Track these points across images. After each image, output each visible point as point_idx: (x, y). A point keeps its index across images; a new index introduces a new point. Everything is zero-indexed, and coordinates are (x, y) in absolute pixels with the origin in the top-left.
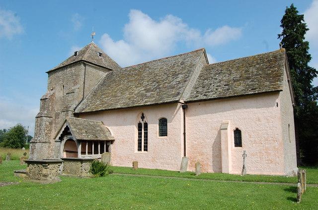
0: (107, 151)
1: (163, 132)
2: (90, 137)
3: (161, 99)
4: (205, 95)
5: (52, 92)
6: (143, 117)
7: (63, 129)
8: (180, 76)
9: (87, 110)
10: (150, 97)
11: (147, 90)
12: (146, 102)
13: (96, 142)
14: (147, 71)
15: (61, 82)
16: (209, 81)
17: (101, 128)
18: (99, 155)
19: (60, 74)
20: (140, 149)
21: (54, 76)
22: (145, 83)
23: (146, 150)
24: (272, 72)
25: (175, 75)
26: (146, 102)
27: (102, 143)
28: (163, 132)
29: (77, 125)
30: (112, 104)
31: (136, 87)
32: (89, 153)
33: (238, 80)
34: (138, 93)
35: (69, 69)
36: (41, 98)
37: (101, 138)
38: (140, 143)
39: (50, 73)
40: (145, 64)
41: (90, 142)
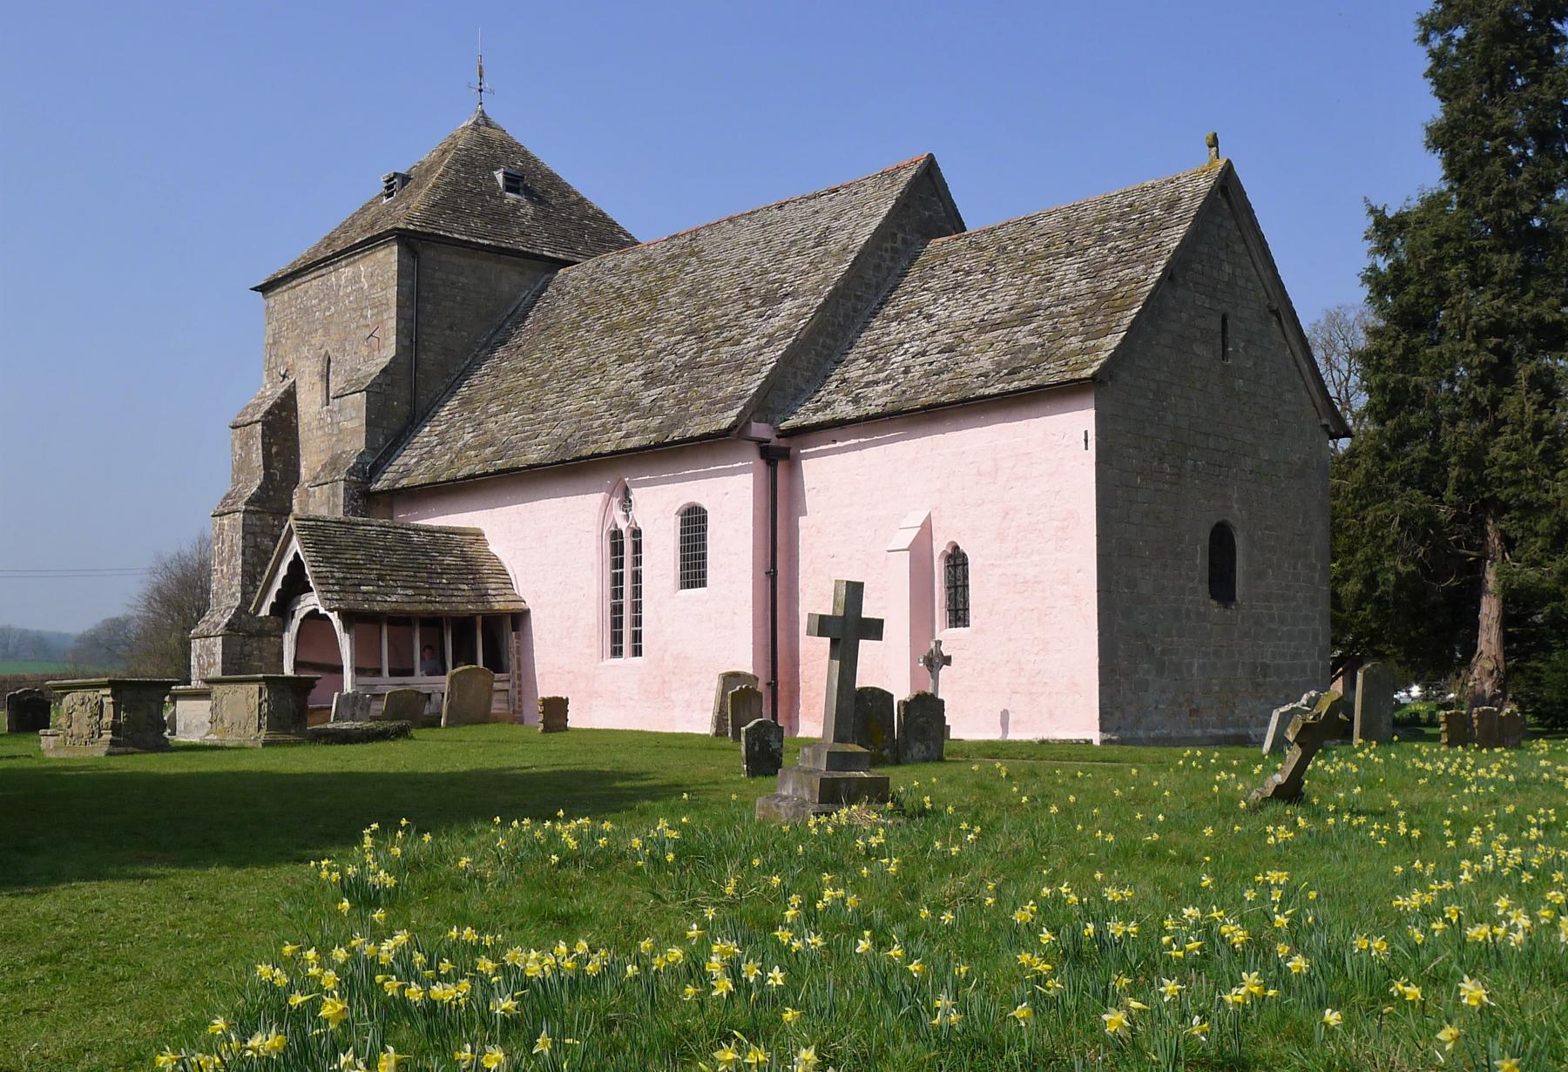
0: (496, 662)
1: (693, 571)
2: (396, 599)
3: (674, 426)
4: (856, 401)
5: (288, 382)
6: (626, 503)
7: (283, 571)
8: (788, 303)
9: (420, 477)
10: (649, 412)
11: (651, 379)
12: (627, 436)
13: (432, 623)
14: (694, 271)
15: (316, 340)
16: (904, 324)
17: (464, 557)
18: (443, 683)
19: (310, 286)
20: (617, 652)
21: (282, 296)
22: (661, 340)
23: (637, 651)
24: (1122, 283)
25: (771, 299)
26: (627, 436)
27: (463, 626)
28: (693, 571)
29: (338, 550)
30: (509, 446)
31: (622, 361)
32: (392, 673)
33: (996, 326)
34: (618, 392)
35: (346, 272)
36: (233, 418)
37: (462, 602)
38: (617, 623)
39: (265, 289)
40: (695, 234)
41: (399, 621)
